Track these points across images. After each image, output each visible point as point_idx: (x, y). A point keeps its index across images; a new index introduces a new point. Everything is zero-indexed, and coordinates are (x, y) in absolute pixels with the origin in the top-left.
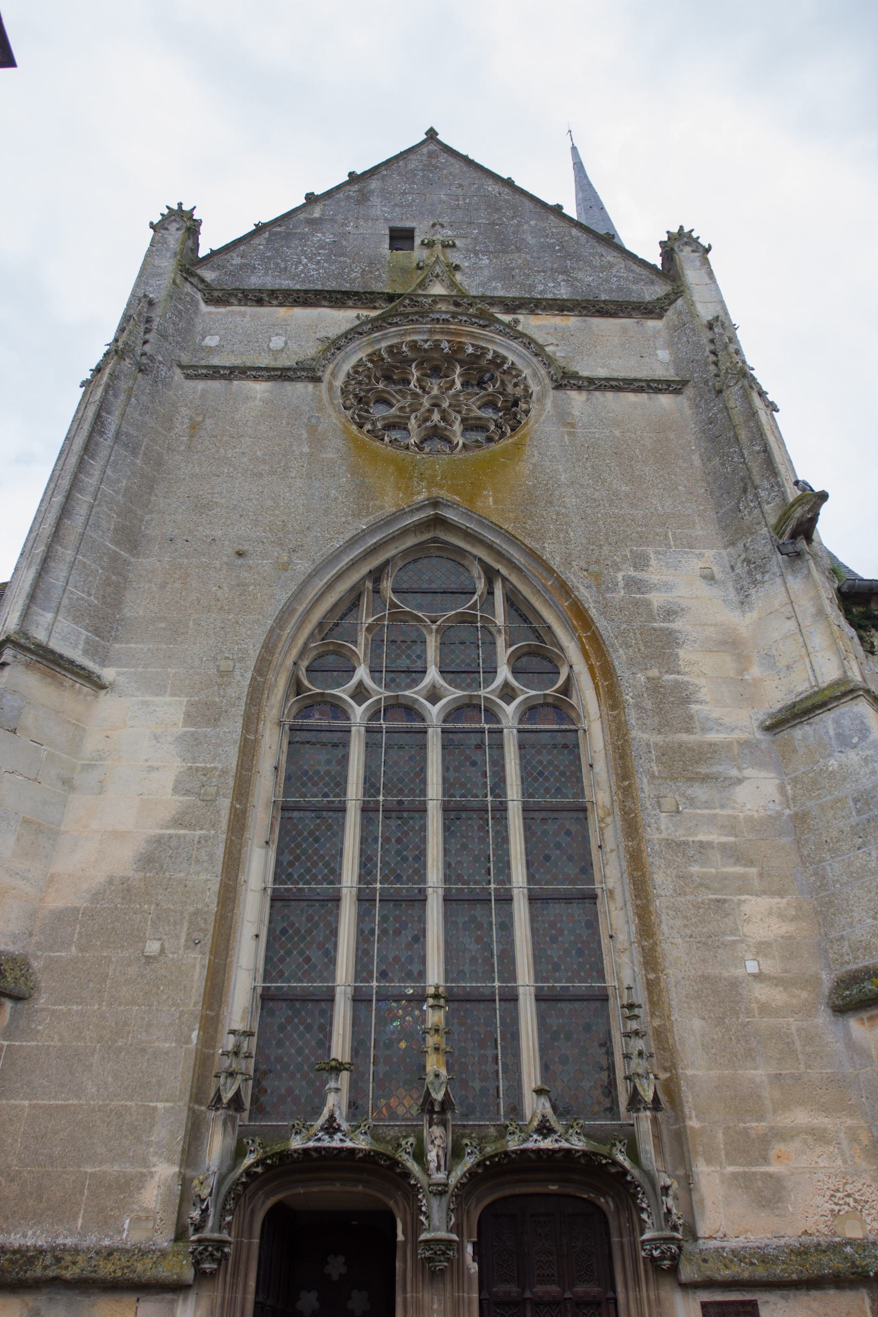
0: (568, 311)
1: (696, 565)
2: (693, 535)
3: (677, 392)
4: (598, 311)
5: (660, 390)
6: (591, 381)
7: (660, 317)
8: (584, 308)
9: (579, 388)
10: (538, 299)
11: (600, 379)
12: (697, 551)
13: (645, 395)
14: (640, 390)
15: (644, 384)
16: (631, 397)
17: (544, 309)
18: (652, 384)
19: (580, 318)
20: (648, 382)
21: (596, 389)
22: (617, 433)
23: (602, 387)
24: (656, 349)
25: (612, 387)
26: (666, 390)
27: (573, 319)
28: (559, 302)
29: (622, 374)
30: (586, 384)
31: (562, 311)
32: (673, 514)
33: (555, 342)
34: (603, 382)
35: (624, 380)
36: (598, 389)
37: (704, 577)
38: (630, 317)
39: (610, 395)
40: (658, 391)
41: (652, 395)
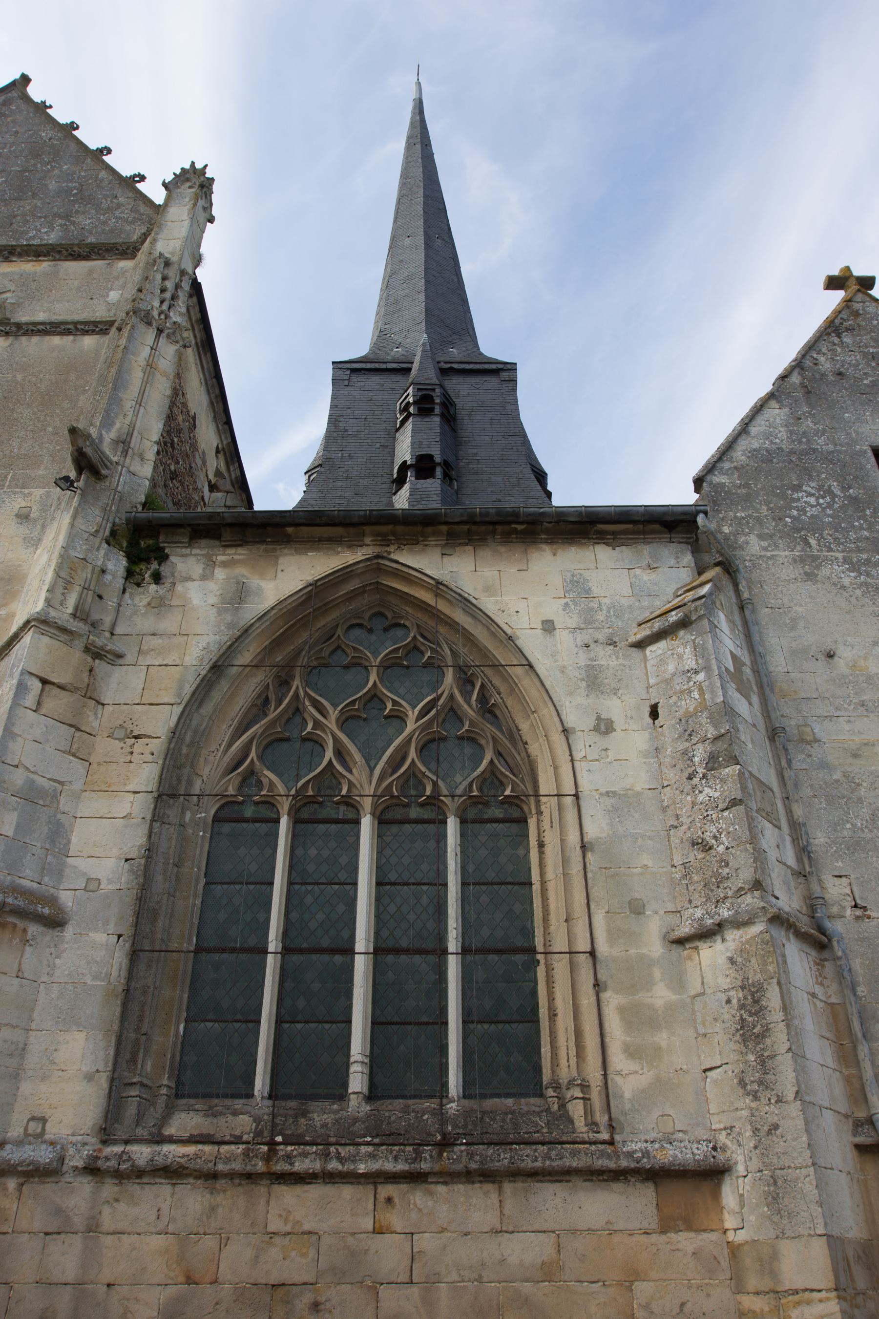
0: (45, 256)
1: (18, 503)
2: (33, 475)
3: (104, 332)
4: (72, 255)
5: (87, 331)
6: (19, 326)
7: (133, 257)
8: (60, 252)
9: (7, 334)
10: (12, 246)
11: (27, 324)
12: (26, 491)
13: (71, 338)
14: (67, 332)
15: (71, 327)
16: (56, 340)
17: (20, 255)
18: (79, 326)
19: (50, 263)
20: (75, 323)
21: (24, 334)
22: (19, 377)
23: (30, 332)
24: (111, 289)
25: (39, 331)
26: (93, 331)
27: (45, 264)
28: (33, 248)
29: (70, 318)
30: (14, 329)
31: (39, 256)
32: (25, 455)
33: (13, 288)
34: (31, 327)
35: (51, 323)
36: (26, 333)
37: (18, 516)
38: (104, 259)
39: (35, 339)
40: (86, 332)
41: (79, 337)
